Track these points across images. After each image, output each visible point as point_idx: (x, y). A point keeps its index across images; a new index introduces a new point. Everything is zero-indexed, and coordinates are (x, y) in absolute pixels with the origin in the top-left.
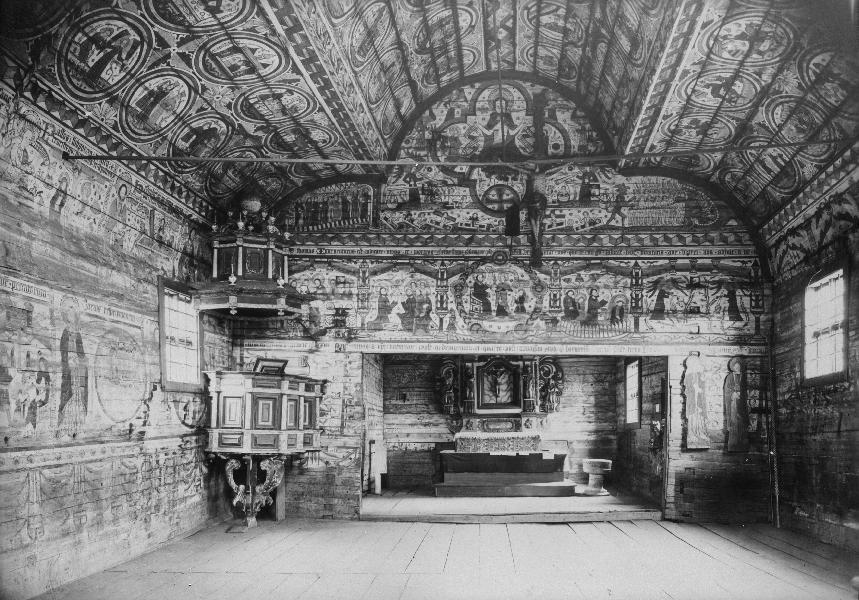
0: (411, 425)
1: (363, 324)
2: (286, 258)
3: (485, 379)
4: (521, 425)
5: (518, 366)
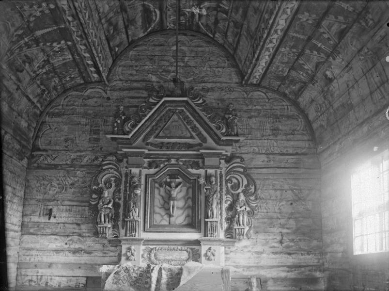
0: (57, 251)
3: (156, 191)
4: (200, 256)
5: (199, 176)
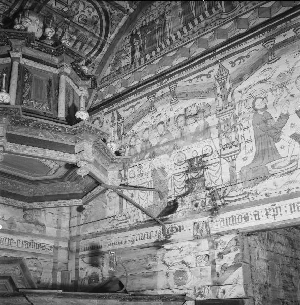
1: (233, 175)
2: (63, 78)
